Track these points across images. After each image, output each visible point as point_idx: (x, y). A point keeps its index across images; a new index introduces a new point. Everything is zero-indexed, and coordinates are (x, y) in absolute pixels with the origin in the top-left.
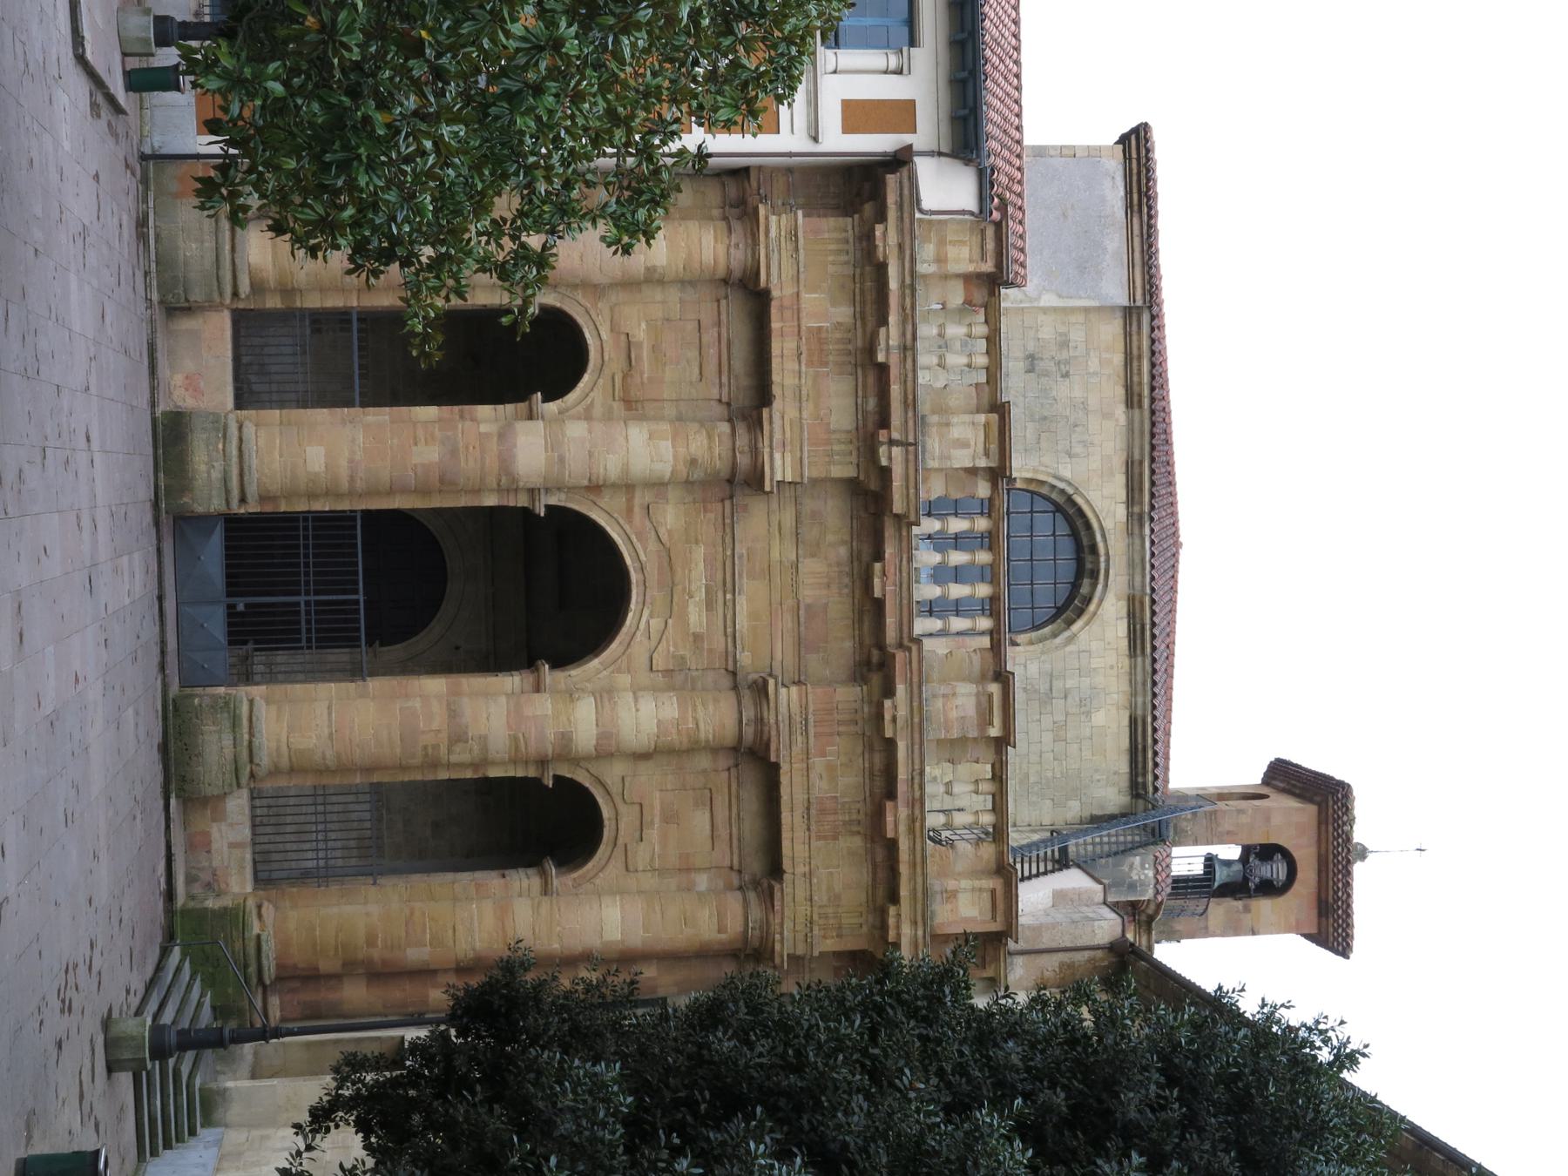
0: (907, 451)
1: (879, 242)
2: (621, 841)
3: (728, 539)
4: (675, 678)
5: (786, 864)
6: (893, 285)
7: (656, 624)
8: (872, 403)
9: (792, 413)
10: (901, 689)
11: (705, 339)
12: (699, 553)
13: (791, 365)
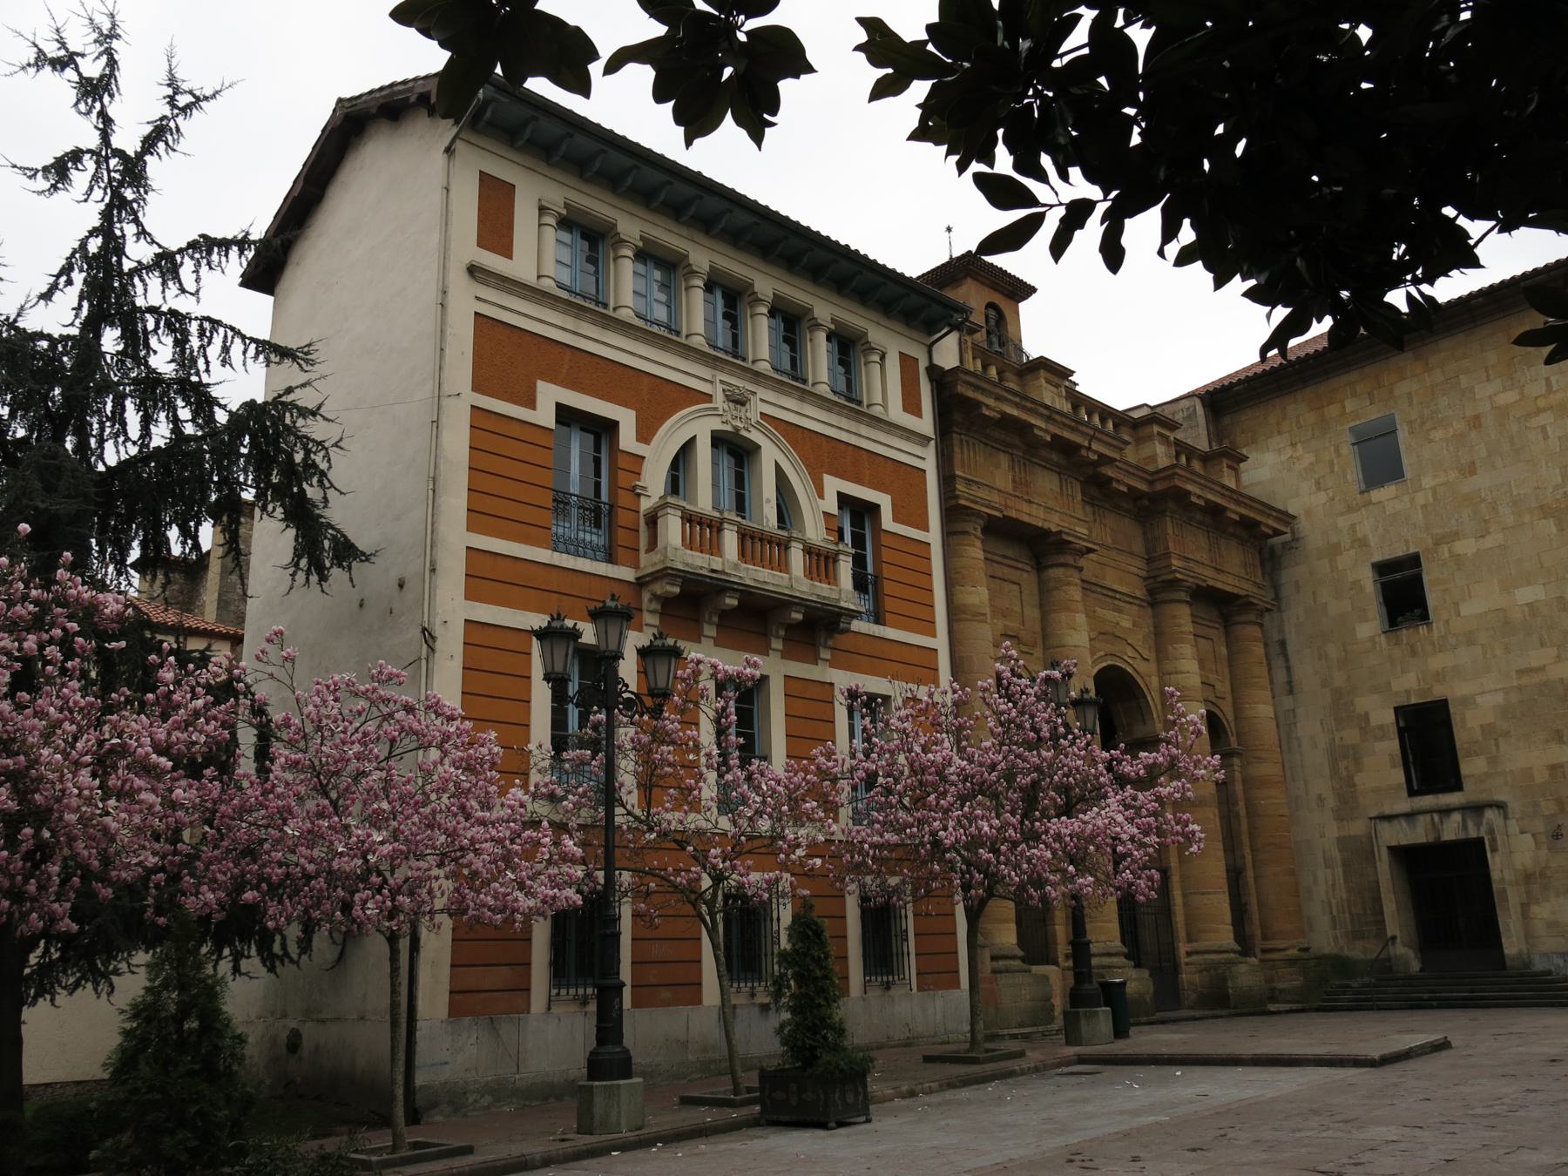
0: (1097, 439)
1: (992, 414)
2: (1214, 700)
3: (1094, 588)
4: (1161, 640)
5: (1235, 591)
6: (1015, 412)
7: (1131, 652)
8: (1054, 457)
9: (1056, 518)
10: (1189, 487)
11: (1000, 575)
12: (1101, 612)
13: (1034, 510)
